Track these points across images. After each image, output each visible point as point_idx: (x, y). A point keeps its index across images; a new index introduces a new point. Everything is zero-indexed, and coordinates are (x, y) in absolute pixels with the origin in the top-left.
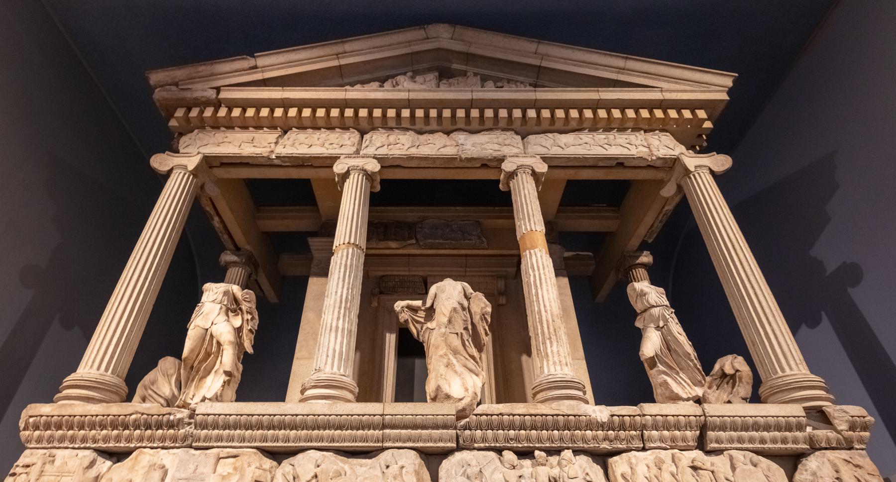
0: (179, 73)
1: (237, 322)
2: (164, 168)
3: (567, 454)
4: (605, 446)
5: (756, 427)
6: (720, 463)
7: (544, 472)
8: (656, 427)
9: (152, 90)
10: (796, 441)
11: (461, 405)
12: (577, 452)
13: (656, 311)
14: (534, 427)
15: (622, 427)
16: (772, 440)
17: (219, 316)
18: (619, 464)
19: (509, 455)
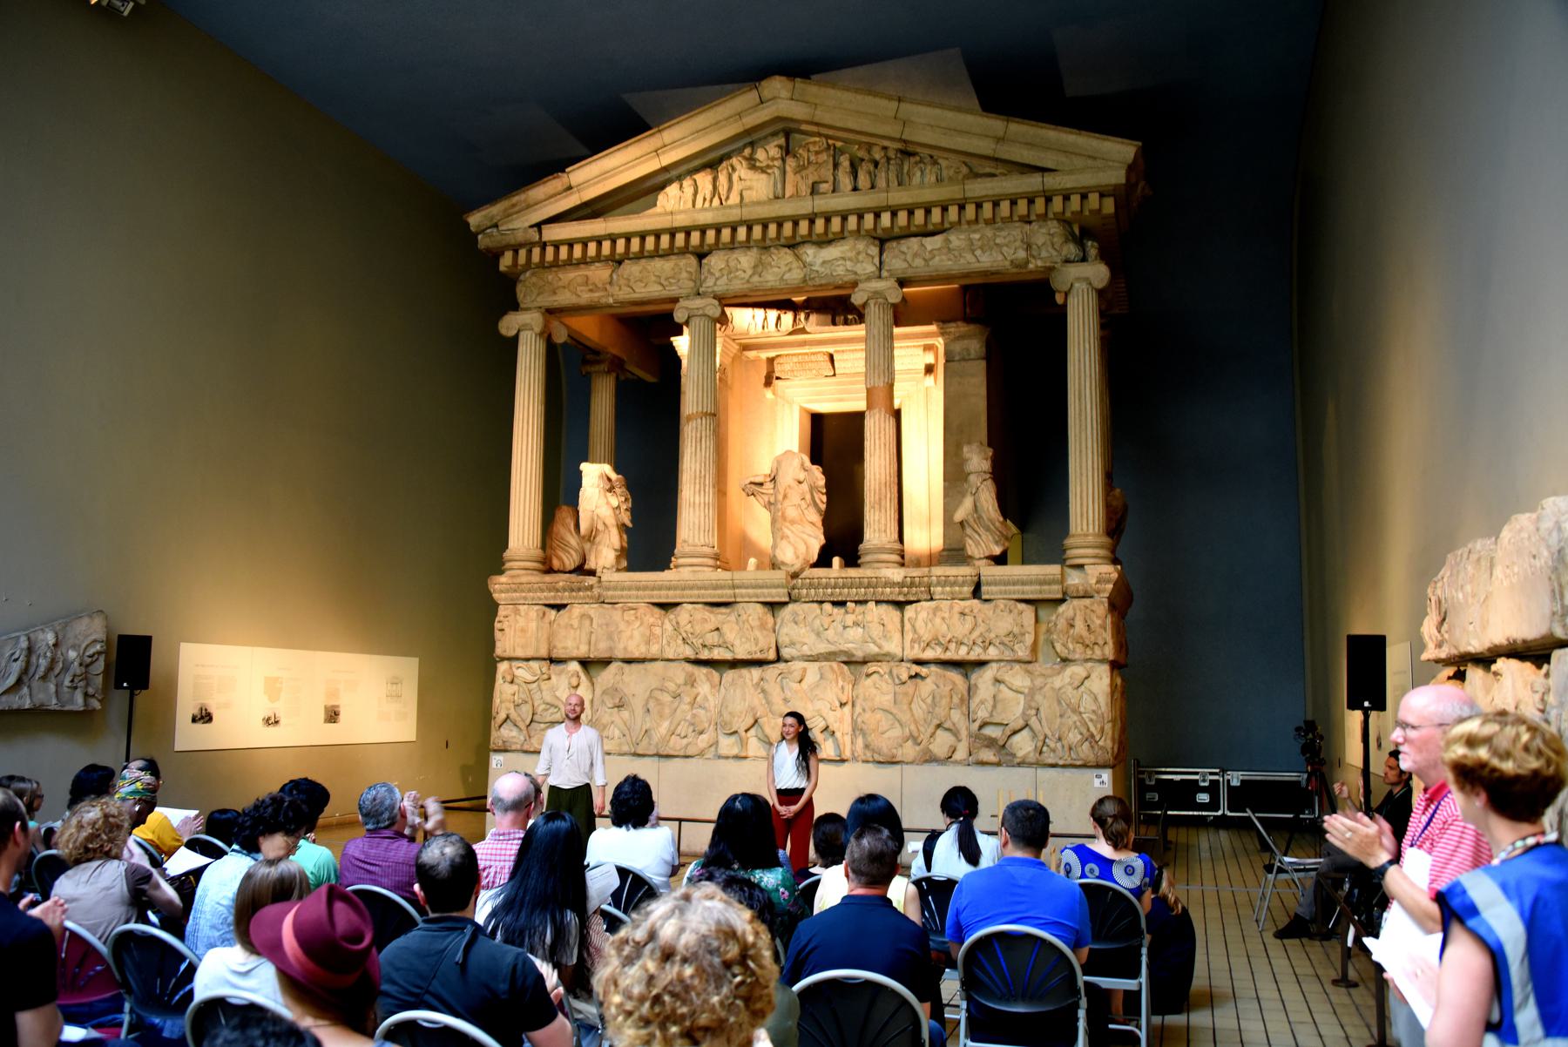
0: (495, 210)
1: (615, 502)
2: (512, 333)
3: (871, 605)
4: (901, 598)
5: (1023, 583)
6: (987, 606)
7: (850, 619)
8: (938, 584)
9: (473, 237)
10: (1054, 592)
11: (792, 570)
12: (878, 602)
13: (972, 478)
14: (844, 587)
15: (912, 585)
16: (1032, 592)
17: (599, 491)
18: (910, 611)
19: (827, 606)
